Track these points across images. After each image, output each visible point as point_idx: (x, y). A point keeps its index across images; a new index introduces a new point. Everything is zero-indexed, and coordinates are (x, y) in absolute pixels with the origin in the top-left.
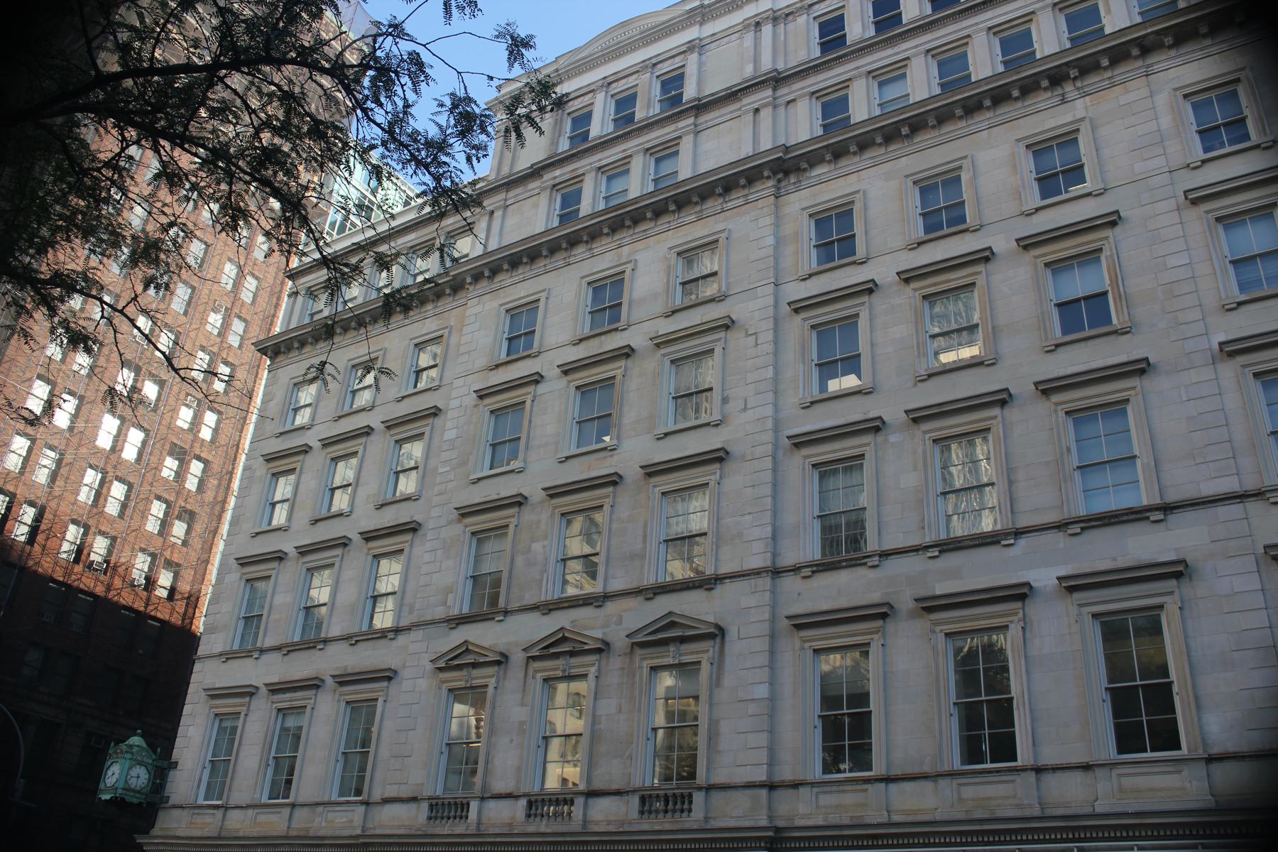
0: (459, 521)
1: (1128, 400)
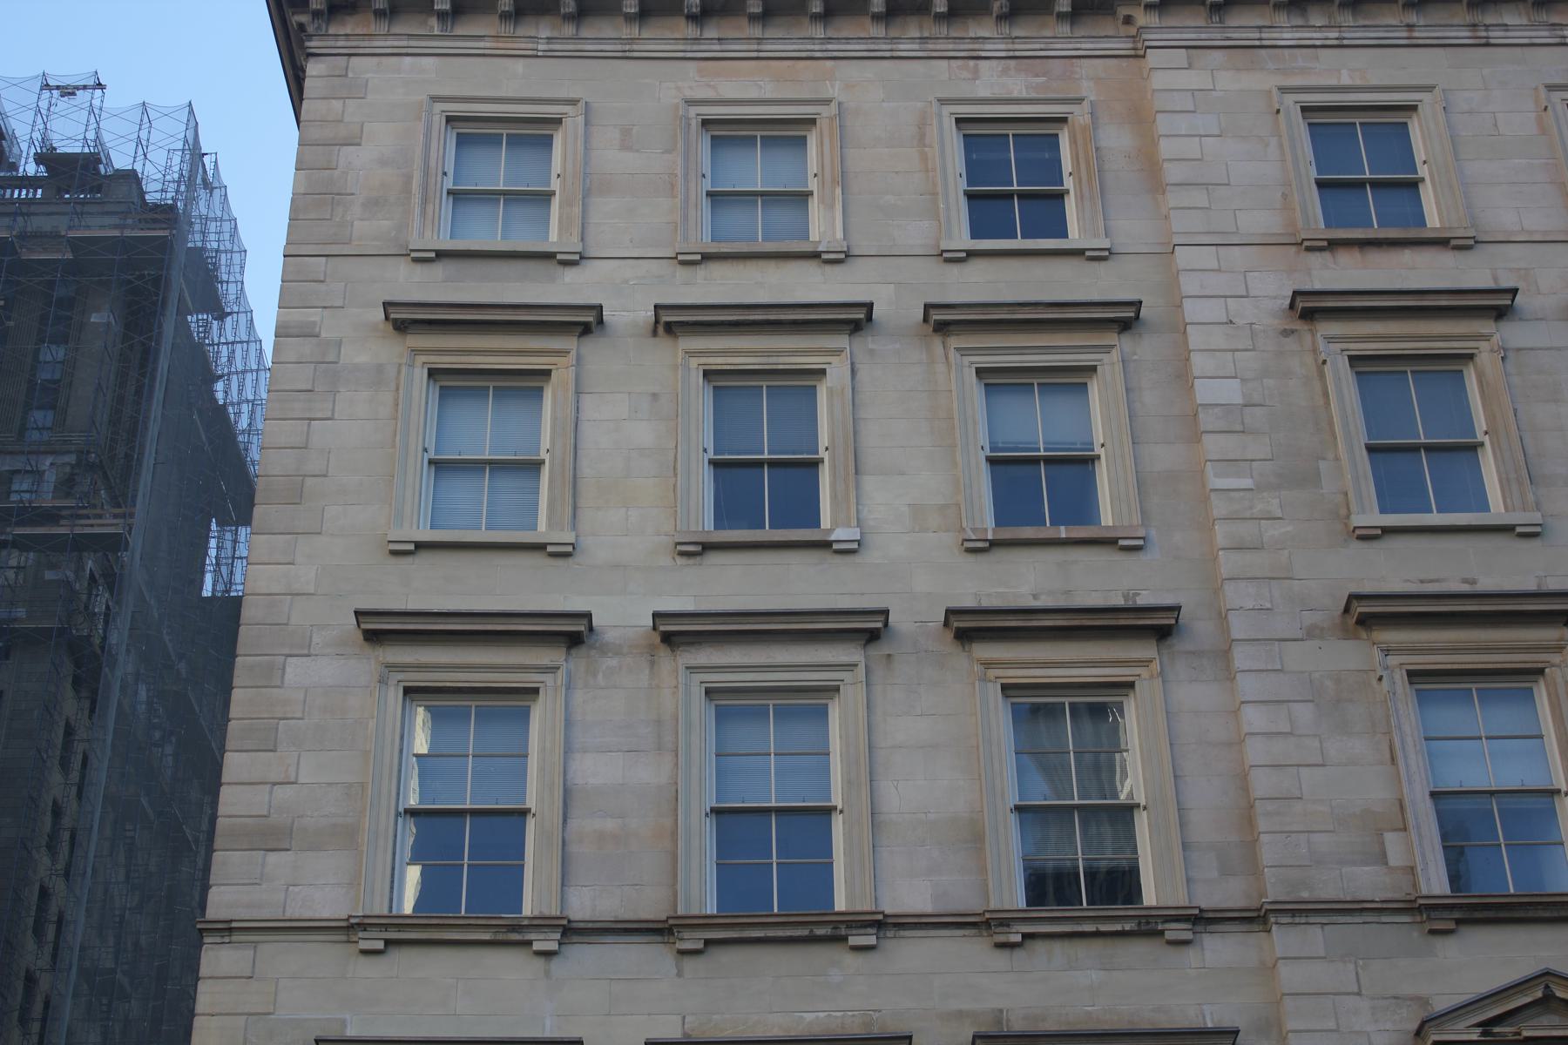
0: (1347, 634)
1: (1131, 685)
